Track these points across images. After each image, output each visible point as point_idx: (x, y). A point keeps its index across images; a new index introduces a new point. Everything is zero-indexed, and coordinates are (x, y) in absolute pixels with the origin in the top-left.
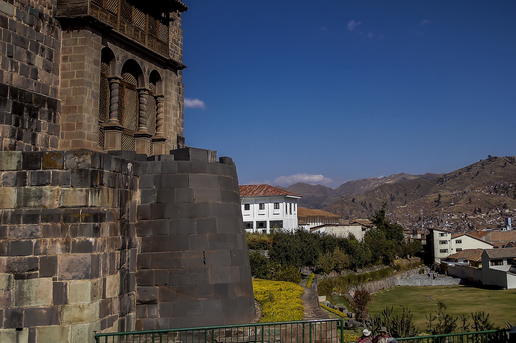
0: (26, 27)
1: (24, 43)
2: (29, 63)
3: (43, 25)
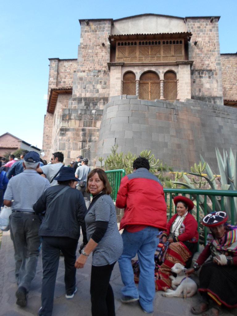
0: (92, 77)
1: (91, 83)
2: (94, 88)
3: (101, 74)
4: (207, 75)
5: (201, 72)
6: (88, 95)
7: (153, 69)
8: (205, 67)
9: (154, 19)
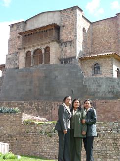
4: (69, 45)
5: (66, 43)
7: (39, 48)
8: (68, 39)
9: (46, 14)
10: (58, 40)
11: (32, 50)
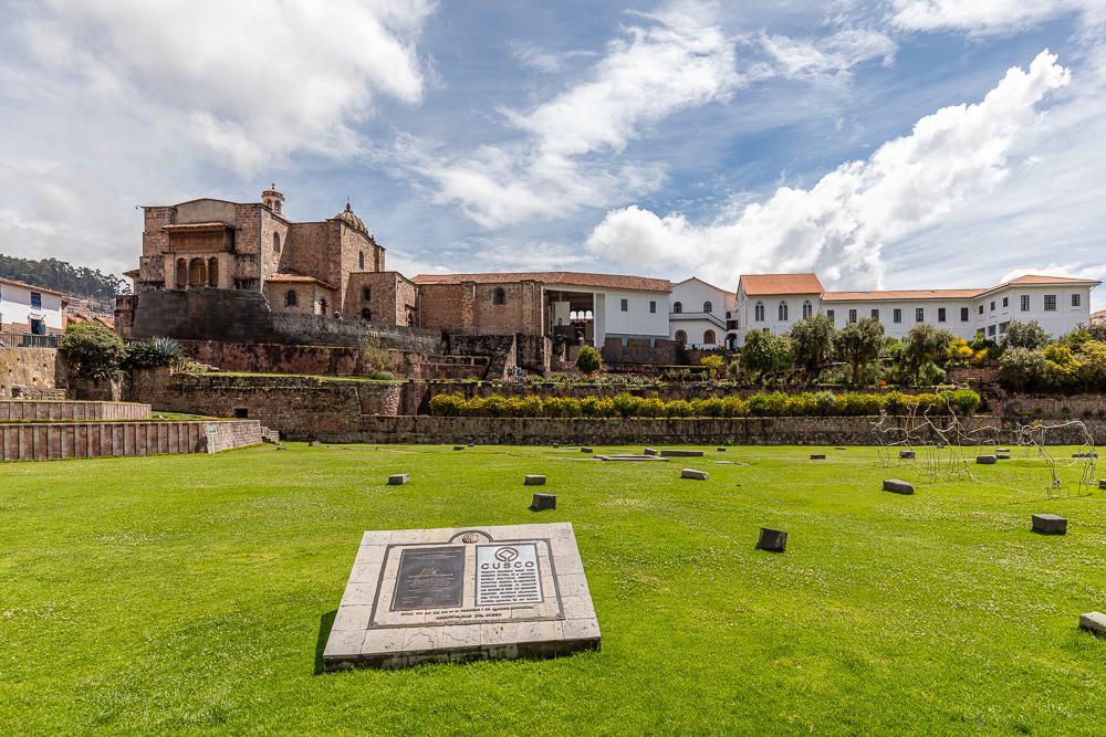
6: (153, 279)
7: (199, 256)
10: (232, 250)
11: (187, 258)
